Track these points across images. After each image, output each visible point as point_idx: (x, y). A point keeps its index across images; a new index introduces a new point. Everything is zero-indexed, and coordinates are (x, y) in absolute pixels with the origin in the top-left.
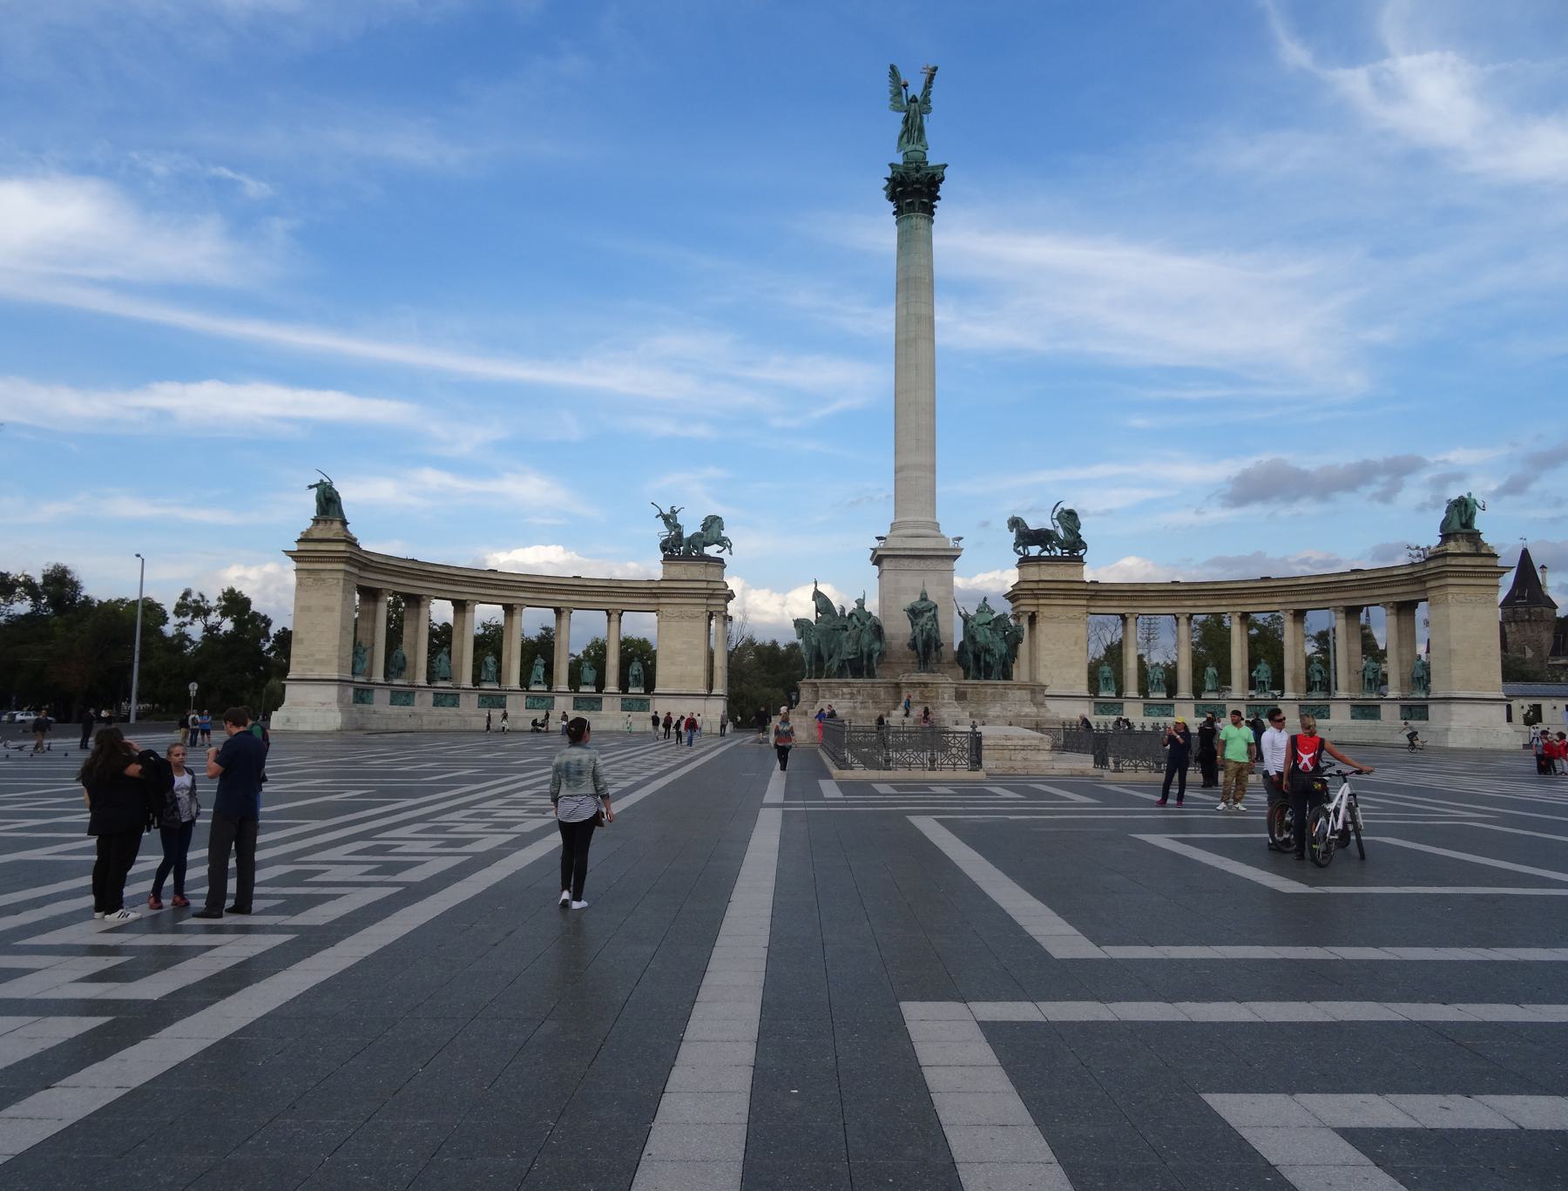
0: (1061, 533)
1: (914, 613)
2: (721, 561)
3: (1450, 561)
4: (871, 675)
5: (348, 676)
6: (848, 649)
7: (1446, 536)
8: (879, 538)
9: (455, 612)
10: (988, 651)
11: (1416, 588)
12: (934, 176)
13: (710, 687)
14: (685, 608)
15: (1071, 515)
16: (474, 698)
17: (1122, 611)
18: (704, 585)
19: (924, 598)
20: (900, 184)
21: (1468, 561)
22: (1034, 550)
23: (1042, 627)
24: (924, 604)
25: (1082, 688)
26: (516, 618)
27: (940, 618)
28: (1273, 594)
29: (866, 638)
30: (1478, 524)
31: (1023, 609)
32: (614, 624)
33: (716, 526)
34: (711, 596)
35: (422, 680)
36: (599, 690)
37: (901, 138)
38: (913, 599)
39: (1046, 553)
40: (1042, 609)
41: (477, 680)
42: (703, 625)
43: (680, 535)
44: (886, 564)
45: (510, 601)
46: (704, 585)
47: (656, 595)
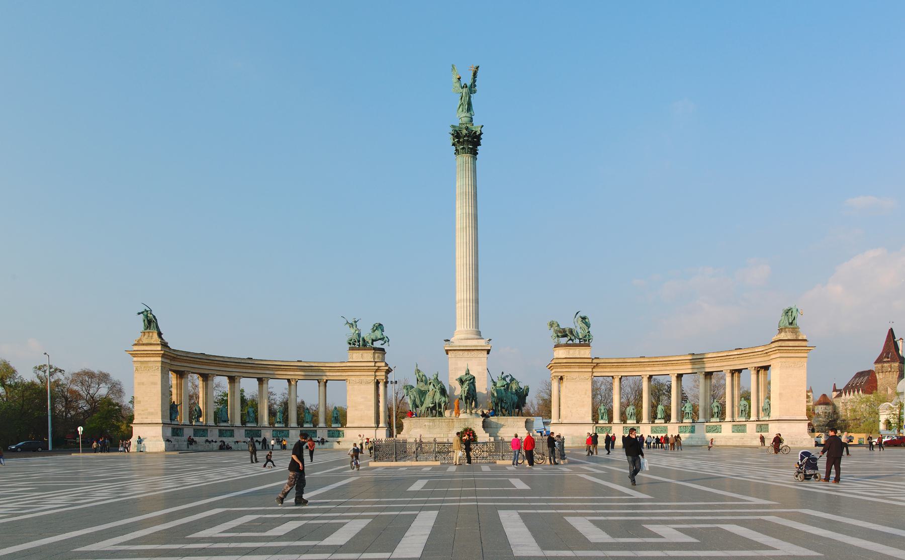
2: (383, 350)
4: (441, 414)
5: (169, 421)
6: (428, 403)
9: (230, 382)
10: (502, 401)
11: (766, 358)
13: (378, 422)
14: (362, 378)
15: (584, 318)
16: (243, 431)
18: (373, 364)
21: (791, 343)
22: (564, 340)
25: (589, 419)
26: (265, 386)
27: (476, 384)
29: (438, 395)
30: (798, 322)
32: (322, 388)
34: (376, 371)
35: (211, 422)
36: (315, 426)
38: (462, 373)
39: (570, 342)
40: (565, 374)
41: (243, 422)
42: (372, 387)
43: (359, 335)
44: (450, 353)
45: (261, 376)
46: (373, 364)
47: (344, 371)
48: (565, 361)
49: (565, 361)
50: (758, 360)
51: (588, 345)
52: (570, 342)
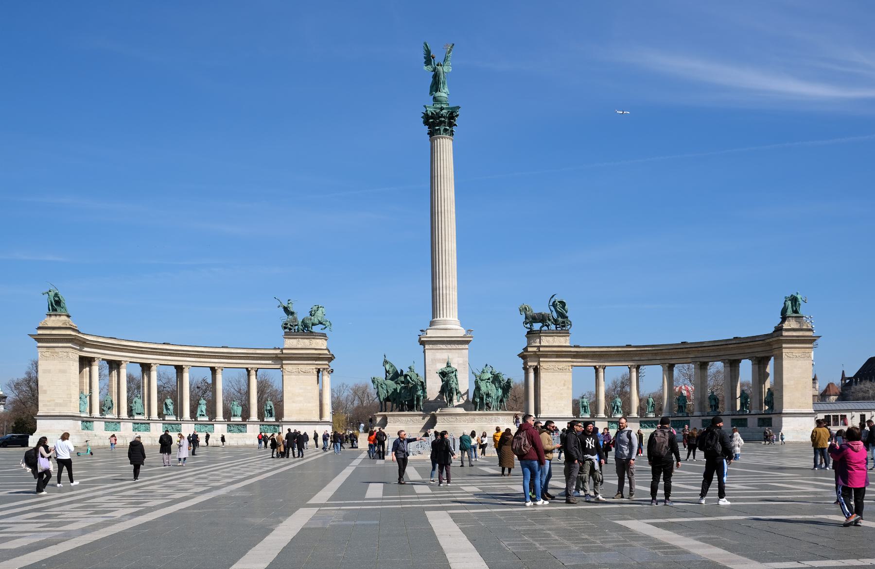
0: (555, 315)
1: (443, 374)
3: (785, 333)
7: (784, 318)
8: (422, 331)
11: (768, 348)
12: (452, 113)
17: (594, 364)
19: (448, 366)
20: (432, 118)
22: (537, 326)
23: (543, 375)
24: (449, 369)
28: (687, 352)
31: (529, 364)
33: (319, 312)
37: (432, 87)
48: (541, 349)
49: (541, 349)
50: (759, 349)
51: (567, 333)
52: (545, 328)
